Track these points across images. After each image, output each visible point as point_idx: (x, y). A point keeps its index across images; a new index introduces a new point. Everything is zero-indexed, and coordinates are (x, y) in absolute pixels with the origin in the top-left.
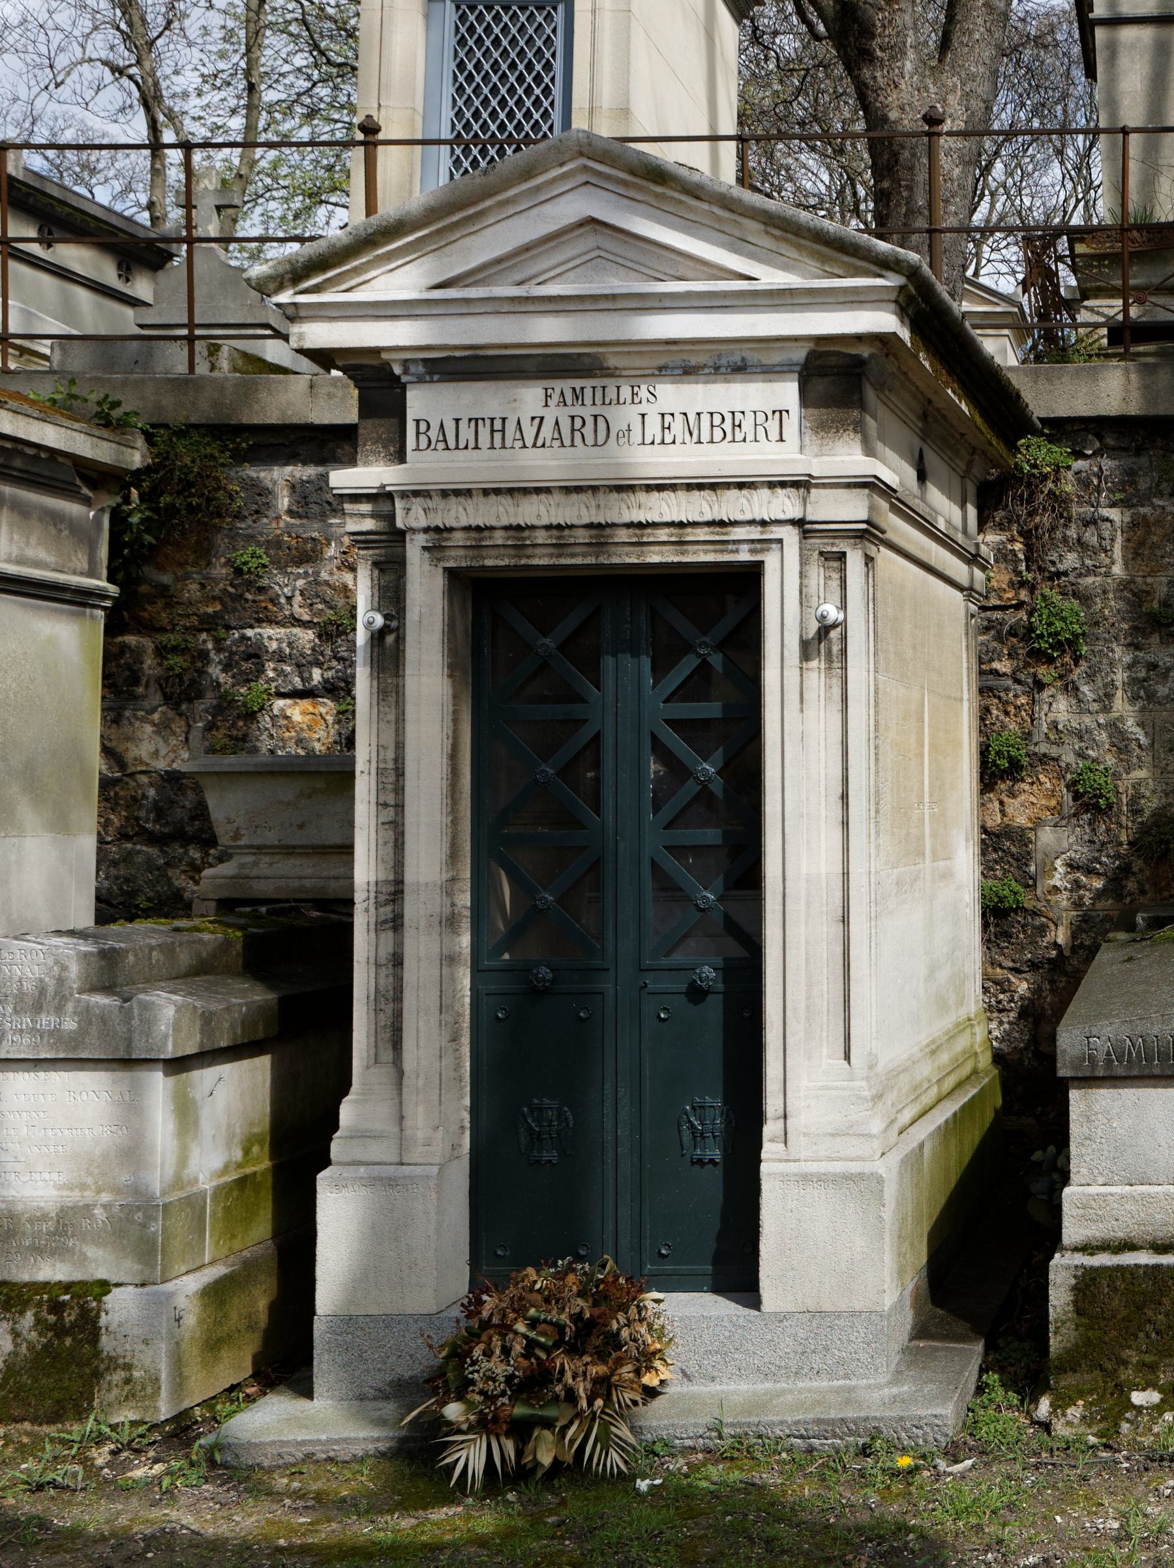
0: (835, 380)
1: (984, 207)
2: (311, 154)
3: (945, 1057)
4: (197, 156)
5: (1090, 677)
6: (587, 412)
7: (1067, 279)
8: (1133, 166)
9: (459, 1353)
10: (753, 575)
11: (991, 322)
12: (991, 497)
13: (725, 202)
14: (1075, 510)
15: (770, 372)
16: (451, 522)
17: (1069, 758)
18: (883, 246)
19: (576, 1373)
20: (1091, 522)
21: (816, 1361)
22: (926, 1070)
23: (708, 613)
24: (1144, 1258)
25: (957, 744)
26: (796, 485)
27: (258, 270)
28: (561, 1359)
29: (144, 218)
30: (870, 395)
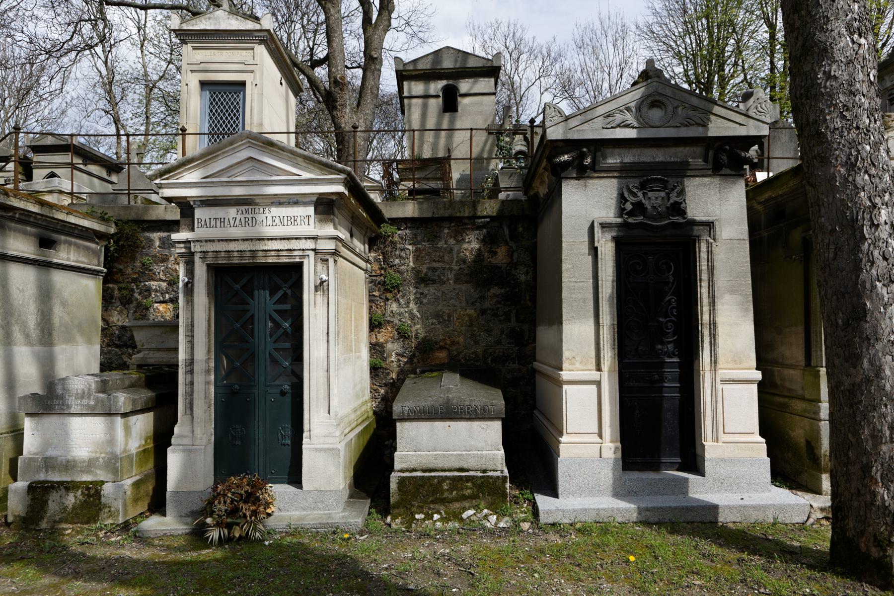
0: (325, 207)
1: (371, 153)
2: (166, 138)
3: (359, 413)
4: (131, 138)
5: (403, 297)
6: (250, 216)
7: (396, 176)
8: (416, 141)
9: (211, 503)
10: (300, 266)
11: (373, 189)
12: (372, 242)
13: (292, 152)
14: (398, 246)
15: (305, 204)
16: (208, 250)
17: (396, 321)
18: (340, 166)
19: (246, 509)
20: (403, 250)
21: (319, 505)
22: (353, 416)
23: (289, 275)
24: (419, 474)
25: (362, 318)
26: (313, 238)
27: (149, 173)
28: (242, 505)
29: (115, 157)
30: (336, 211)
